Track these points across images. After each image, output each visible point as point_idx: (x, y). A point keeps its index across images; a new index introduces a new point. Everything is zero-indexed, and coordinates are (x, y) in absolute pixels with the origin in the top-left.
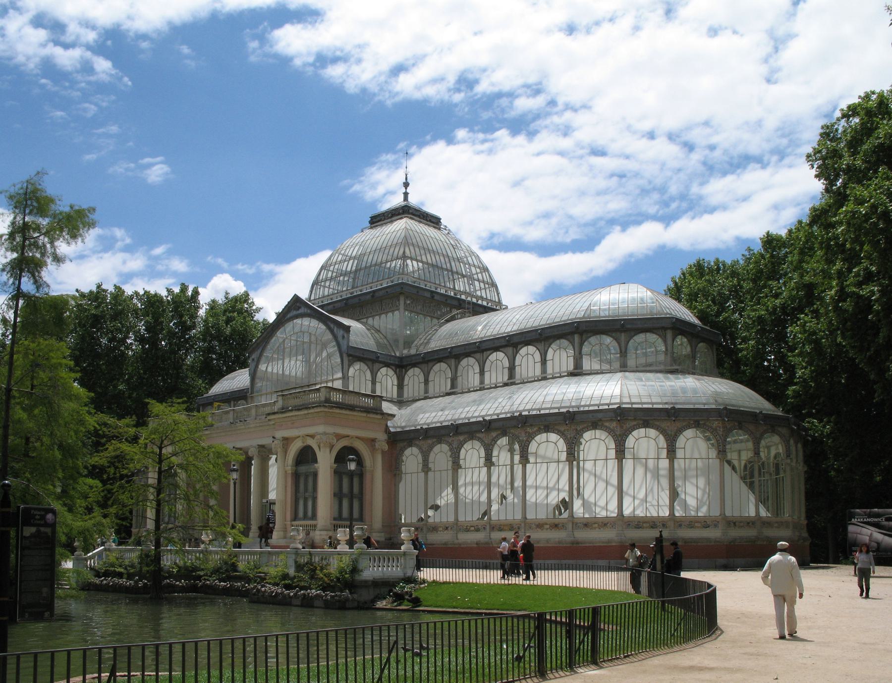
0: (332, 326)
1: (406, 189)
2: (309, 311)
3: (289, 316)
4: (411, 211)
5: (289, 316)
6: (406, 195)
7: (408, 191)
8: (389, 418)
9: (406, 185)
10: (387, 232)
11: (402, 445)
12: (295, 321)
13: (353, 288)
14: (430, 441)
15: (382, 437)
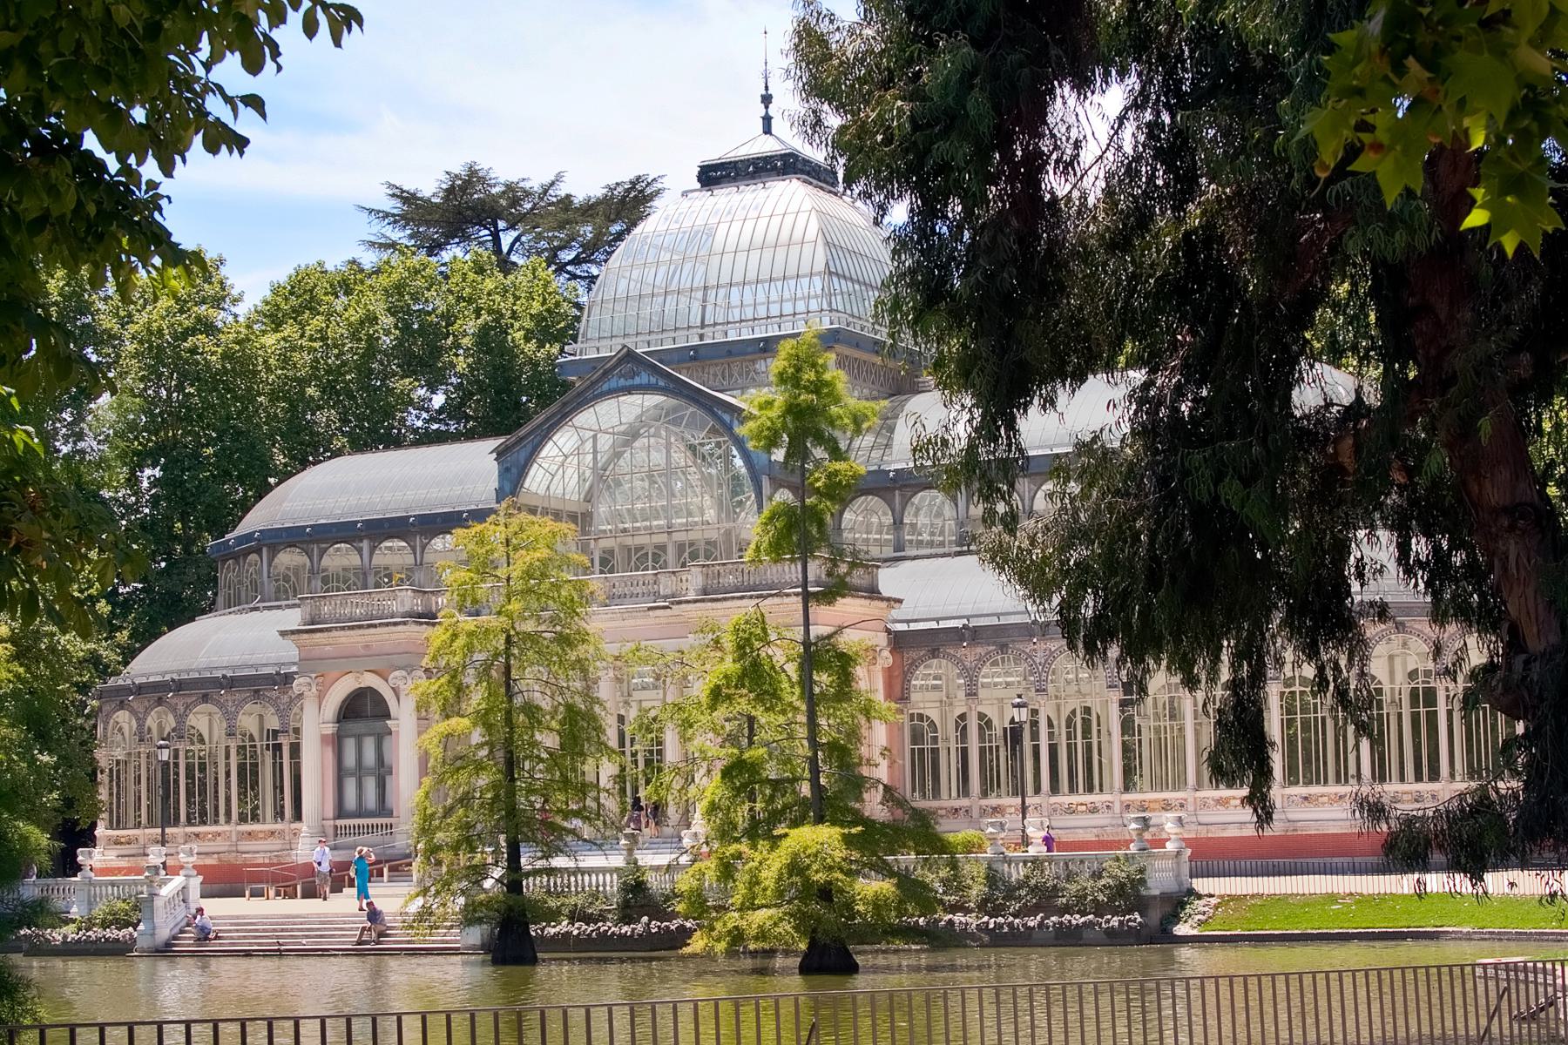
0: (727, 418)
1: (767, 107)
2: (661, 383)
3: (605, 387)
4: (800, 166)
5: (605, 387)
6: (767, 120)
7: (771, 112)
8: (897, 605)
9: (767, 100)
10: (767, 211)
11: (914, 654)
12: (621, 399)
13: (703, 326)
14: (980, 650)
15: (882, 640)
